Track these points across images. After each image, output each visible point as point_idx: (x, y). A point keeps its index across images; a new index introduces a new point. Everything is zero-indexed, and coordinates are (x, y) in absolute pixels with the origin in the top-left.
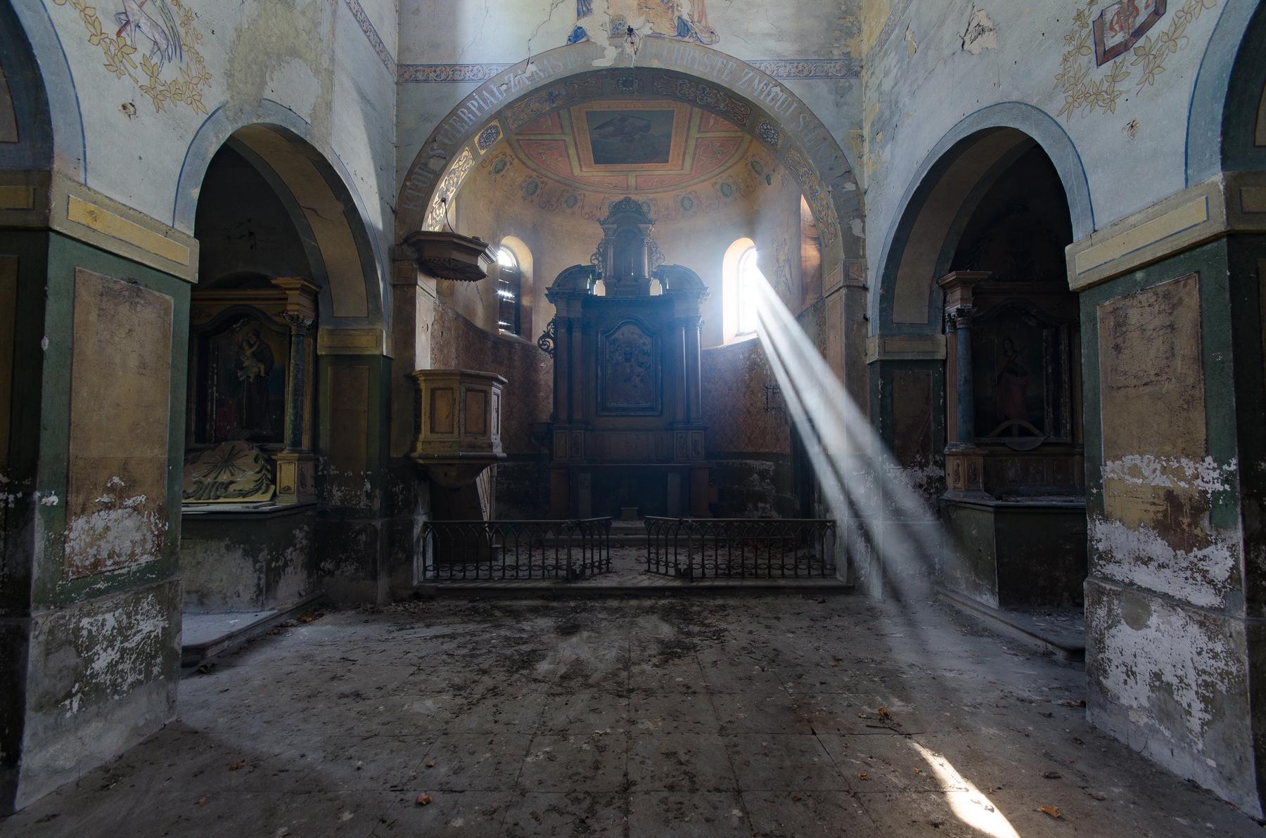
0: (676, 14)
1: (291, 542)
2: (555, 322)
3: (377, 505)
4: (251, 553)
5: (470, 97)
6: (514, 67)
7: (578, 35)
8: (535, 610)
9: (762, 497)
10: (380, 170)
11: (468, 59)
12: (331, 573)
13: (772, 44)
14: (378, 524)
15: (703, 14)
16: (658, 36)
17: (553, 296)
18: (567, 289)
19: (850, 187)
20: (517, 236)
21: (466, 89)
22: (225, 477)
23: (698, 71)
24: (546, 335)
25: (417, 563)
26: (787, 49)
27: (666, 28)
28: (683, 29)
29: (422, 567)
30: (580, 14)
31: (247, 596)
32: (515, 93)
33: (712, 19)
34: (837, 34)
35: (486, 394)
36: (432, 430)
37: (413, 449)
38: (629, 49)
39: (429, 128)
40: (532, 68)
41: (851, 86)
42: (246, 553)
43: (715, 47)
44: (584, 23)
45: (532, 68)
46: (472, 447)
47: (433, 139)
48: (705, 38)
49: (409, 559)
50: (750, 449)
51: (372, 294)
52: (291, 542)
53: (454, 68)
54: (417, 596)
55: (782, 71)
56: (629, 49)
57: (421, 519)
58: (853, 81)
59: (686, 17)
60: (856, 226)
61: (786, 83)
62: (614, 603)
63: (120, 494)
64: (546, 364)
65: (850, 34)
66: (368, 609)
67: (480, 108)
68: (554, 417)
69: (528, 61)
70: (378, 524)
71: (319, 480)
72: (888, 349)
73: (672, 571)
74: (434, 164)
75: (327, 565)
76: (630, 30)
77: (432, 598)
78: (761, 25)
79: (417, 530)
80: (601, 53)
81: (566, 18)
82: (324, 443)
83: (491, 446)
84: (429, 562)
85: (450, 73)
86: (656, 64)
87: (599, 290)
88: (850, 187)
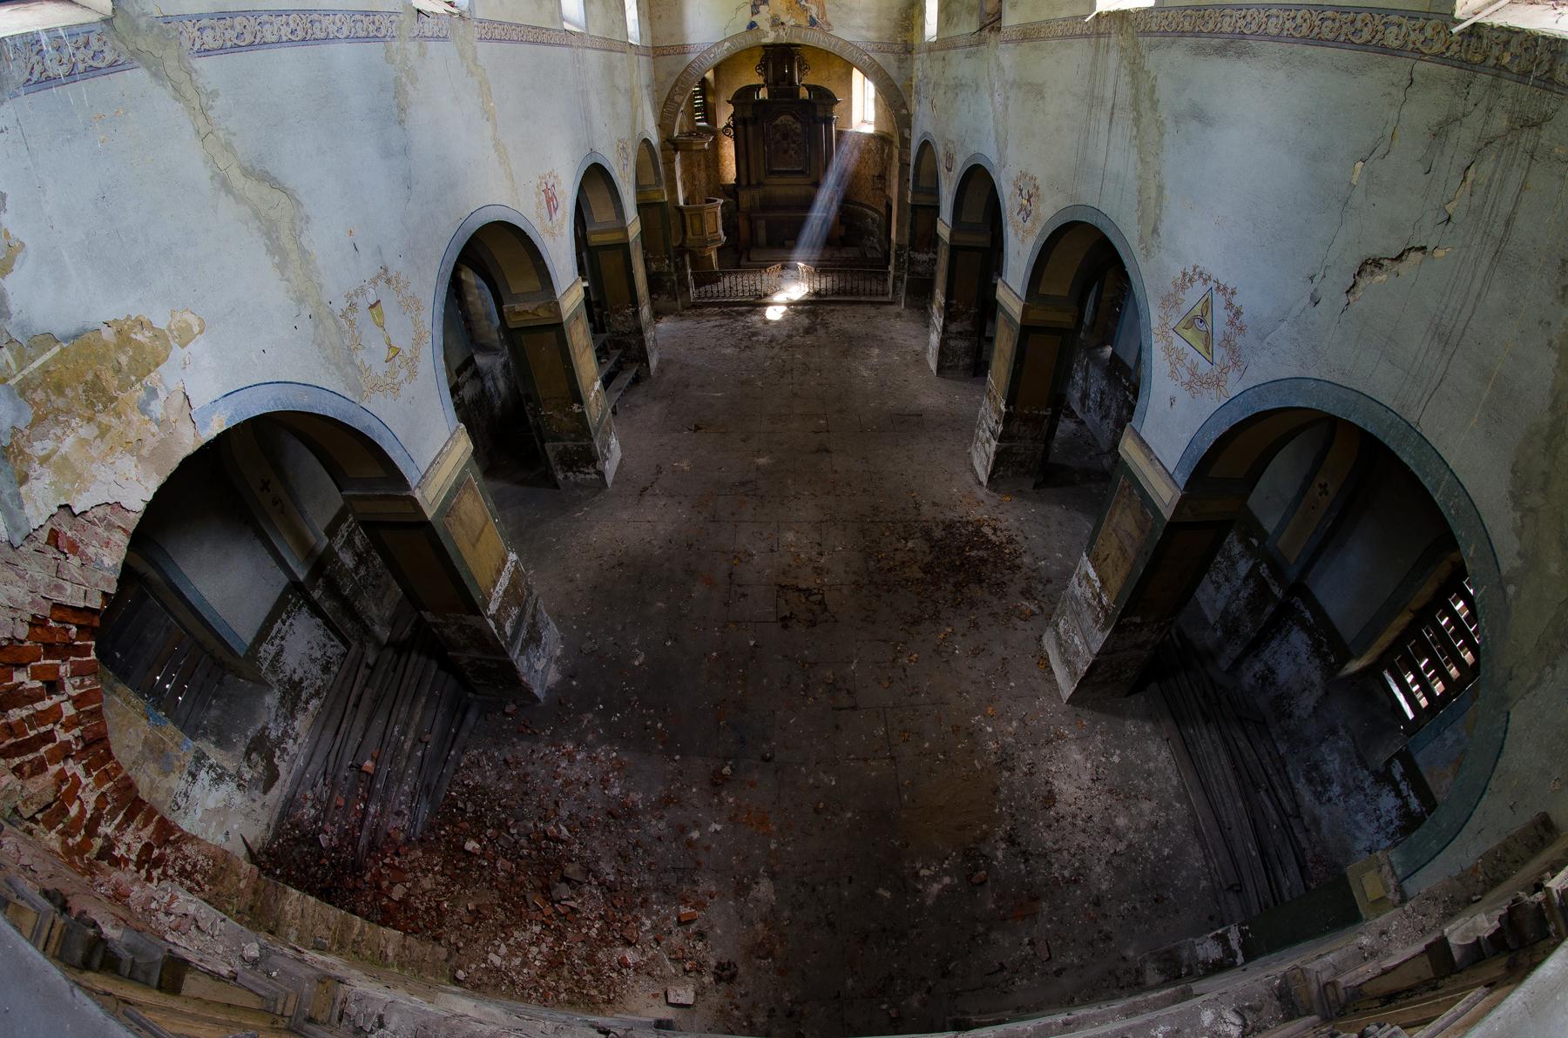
6: (717, 44)
7: (752, 25)
9: (871, 233)
10: (654, 110)
11: (690, 41)
13: (863, 32)
15: (824, 14)
21: (692, 57)
23: (822, 45)
26: (872, 35)
27: (804, 23)
28: (813, 23)
30: (753, 14)
33: (829, 17)
38: (782, 33)
44: (755, 19)
45: (727, 44)
47: (676, 85)
51: (657, 173)
53: (684, 46)
56: (782, 33)
60: (907, 131)
78: (858, 21)
80: (766, 35)
81: (745, 16)
85: (682, 49)
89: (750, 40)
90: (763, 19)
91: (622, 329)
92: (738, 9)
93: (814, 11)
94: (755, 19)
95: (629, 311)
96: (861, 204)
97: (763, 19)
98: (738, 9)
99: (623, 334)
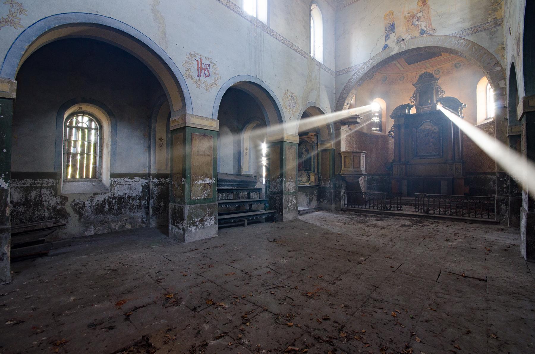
0: (420, 28)
1: (313, 194)
2: (394, 126)
3: (332, 186)
4: (306, 195)
5: (354, 75)
6: (366, 63)
7: (386, 46)
8: (371, 216)
10: (331, 102)
11: (353, 65)
12: (322, 202)
14: (332, 191)
16: (414, 38)
17: (392, 117)
18: (399, 114)
19: (498, 69)
20: (383, 98)
21: (353, 73)
22: (300, 179)
24: (391, 131)
25: (342, 202)
26: (467, 25)
27: (416, 34)
28: (423, 32)
29: (344, 203)
31: (306, 204)
32: (366, 70)
34: (490, 12)
35: (360, 157)
36: (345, 167)
37: (340, 172)
38: (403, 45)
39: (343, 86)
40: (371, 61)
41: (497, 30)
42: (305, 195)
43: (435, 34)
44: (387, 43)
46: (356, 171)
48: (431, 32)
49: (340, 201)
50: (489, 170)
52: (313, 194)
54: (342, 210)
55: (465, 34)
57: (343, 191)
58: (499, 28)
59: (424, 28)
61: (467, 38)
62: (397, 217)
63: (291, 179)
64: (391, 141)
65: (496, 10)
66: (330, 210)
67: (356, 77)
68: (394, 160)
69: (370, 60)
70: (332, 191)
71: (319, 180)
72: (513, 130)
73: (422, 211)
74: (344, 96)
75: (321, 200)
76: (403, 40)
77: (345, 211)
79: (342, 193)
81: (382, 43)
82: (320, 171)
83: (361, 171)
84: (346, 202)
85: (348, 70)
86: (412, 47)
87: (413, 111)
88: (498, 69)
89: (384, 56)
90: (392, 43)
91: (274, 190)
92: (378, 40)
93: (423, 25)
94: (387, 43)
95: (278, 180)
96: (485, 173)
97: (392, 43)
98: (378, 40)
99: (274, 193)
